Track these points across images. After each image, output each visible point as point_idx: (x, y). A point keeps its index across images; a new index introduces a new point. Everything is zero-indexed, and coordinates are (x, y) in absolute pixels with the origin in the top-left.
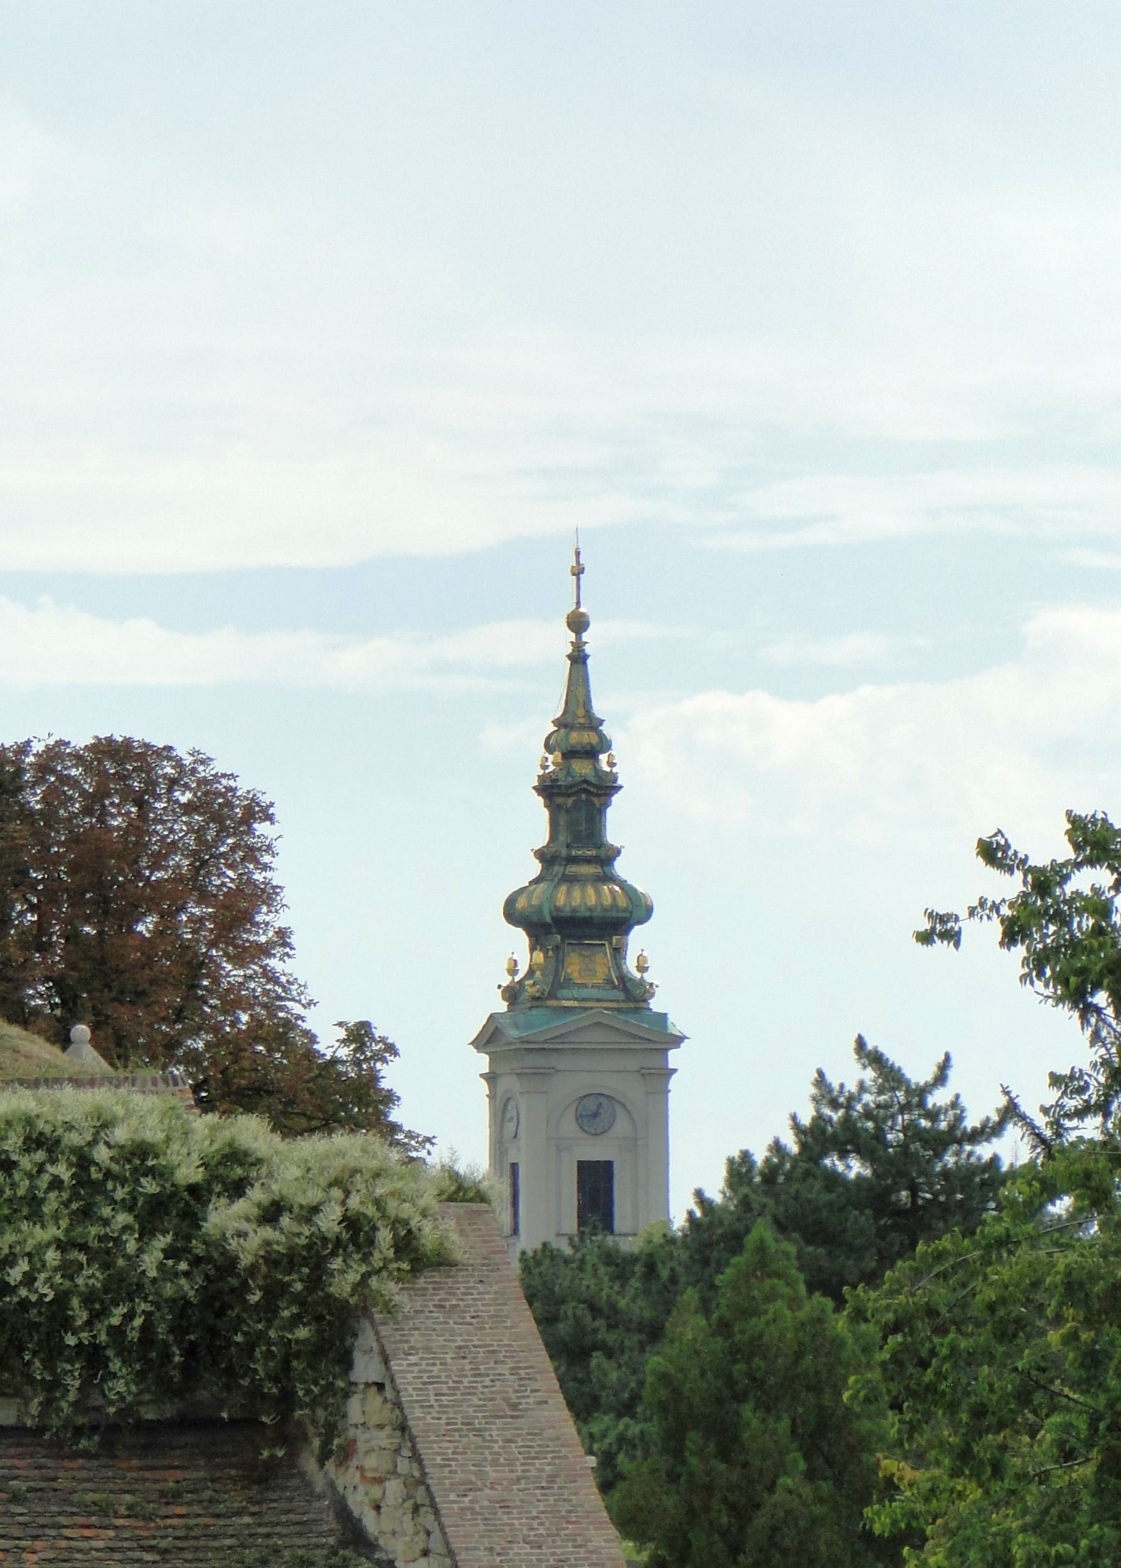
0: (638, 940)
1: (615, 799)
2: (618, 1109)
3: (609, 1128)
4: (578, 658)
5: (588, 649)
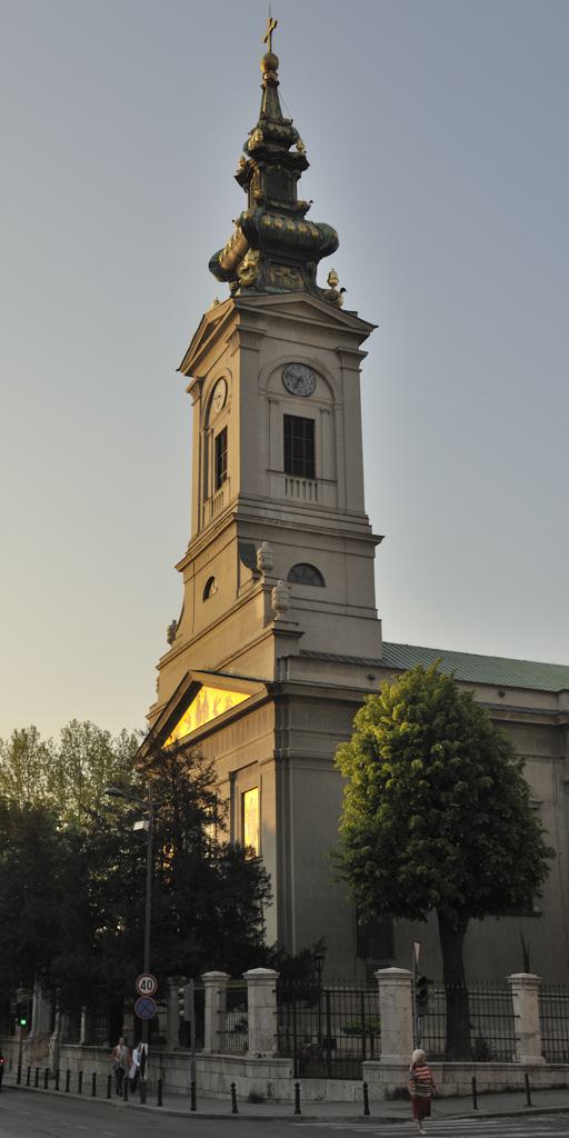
0: (324, 268)
1: (303, 173)
2: (318, 378)
3: (310, 394)
4: (271, 85)
5: (278, 79)
